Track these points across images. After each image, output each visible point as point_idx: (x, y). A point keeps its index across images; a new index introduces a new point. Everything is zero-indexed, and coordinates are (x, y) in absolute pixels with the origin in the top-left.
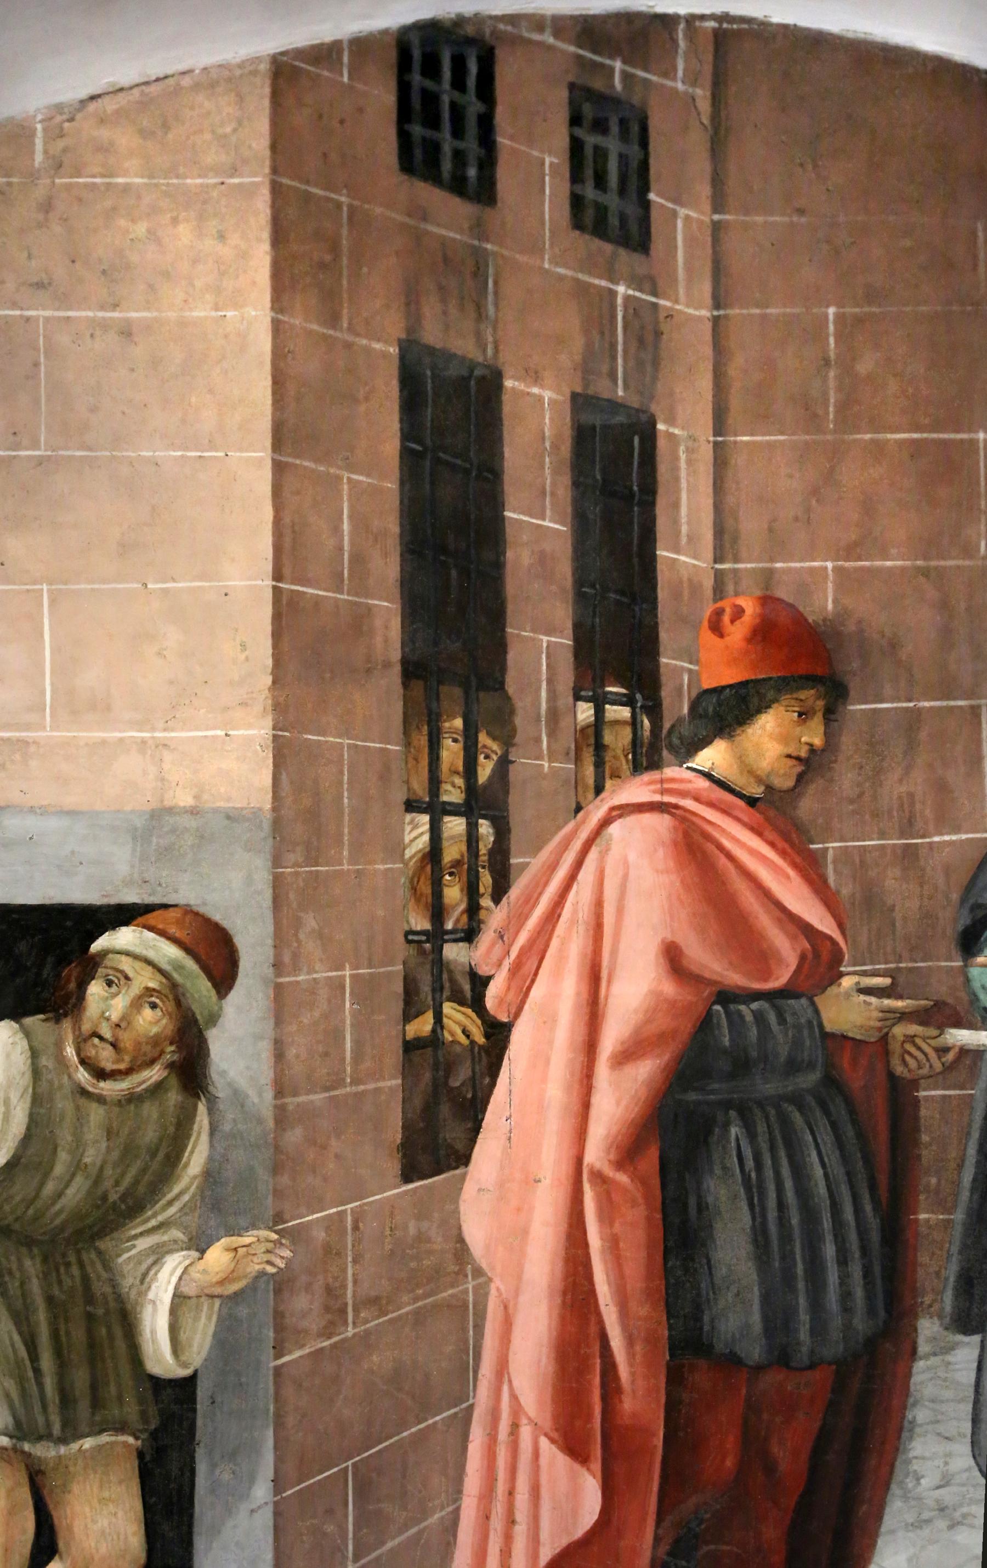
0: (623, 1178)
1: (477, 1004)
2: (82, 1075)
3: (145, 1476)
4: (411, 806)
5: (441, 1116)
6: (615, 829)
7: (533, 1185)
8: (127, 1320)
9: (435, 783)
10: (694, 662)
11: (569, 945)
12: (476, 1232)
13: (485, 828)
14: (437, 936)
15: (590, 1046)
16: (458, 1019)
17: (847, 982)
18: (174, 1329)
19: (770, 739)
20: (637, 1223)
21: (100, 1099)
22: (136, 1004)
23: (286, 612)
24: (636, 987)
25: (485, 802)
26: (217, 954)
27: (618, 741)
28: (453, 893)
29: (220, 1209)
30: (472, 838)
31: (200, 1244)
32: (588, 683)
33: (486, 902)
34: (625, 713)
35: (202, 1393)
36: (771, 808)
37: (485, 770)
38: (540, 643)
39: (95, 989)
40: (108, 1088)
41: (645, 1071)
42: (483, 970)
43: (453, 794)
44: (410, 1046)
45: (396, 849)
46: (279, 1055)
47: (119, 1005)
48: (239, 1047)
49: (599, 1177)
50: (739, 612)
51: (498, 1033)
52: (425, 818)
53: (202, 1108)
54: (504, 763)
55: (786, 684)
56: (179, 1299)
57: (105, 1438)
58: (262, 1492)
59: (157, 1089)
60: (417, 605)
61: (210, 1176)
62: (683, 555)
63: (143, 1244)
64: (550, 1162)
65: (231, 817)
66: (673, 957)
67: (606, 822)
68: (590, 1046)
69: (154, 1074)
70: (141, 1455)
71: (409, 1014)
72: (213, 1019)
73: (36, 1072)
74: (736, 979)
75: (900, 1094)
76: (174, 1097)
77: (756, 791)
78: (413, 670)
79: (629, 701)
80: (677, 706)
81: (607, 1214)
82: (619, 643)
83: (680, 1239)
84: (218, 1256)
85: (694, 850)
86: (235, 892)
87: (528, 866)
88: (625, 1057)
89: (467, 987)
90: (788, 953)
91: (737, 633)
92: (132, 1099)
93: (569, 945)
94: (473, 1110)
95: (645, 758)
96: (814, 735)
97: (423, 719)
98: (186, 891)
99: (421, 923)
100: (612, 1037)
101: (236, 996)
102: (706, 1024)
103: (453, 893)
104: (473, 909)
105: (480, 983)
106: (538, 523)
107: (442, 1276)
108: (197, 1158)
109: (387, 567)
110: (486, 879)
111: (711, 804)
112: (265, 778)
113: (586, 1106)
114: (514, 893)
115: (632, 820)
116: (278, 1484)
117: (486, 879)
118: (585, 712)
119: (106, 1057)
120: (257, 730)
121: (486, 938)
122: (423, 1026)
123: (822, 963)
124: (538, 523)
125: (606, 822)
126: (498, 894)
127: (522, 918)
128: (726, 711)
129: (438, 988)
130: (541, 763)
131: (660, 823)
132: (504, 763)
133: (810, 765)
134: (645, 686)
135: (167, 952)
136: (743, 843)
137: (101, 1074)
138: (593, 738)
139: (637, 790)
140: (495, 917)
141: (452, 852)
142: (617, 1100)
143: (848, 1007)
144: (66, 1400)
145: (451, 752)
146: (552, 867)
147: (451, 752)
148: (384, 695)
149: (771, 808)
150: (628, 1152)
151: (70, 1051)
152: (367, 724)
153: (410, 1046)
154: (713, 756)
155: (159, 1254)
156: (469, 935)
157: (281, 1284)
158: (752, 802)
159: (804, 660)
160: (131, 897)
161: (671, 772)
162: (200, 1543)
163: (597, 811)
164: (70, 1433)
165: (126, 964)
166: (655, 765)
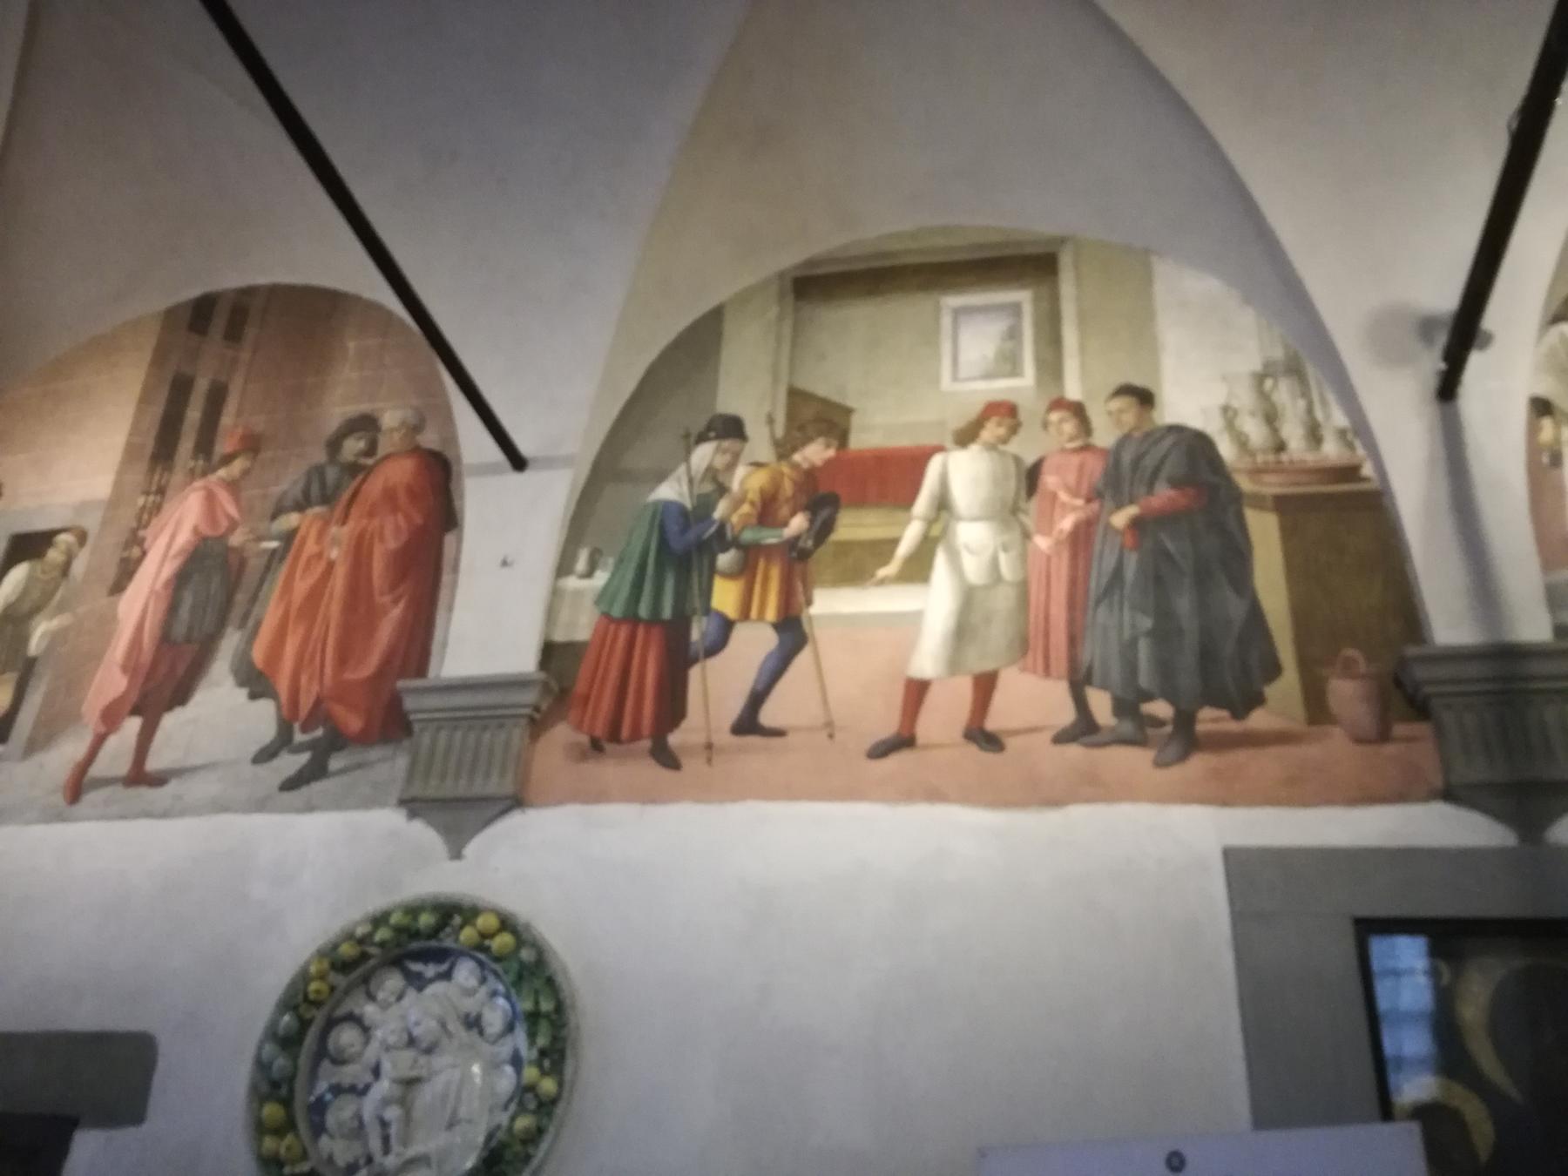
19: (238, 466)
20: (163, 606)
24: (184, 538)
25: (161, 491)
26: (82, 537)
27: (198, 471)
28: (146, 516)
32: (195, 457)
36: (233, 486)
38: (186, 445)
43: (154, 488)
48: (79, 567)
51: (144, 554)
64: (146, 590)
66: (196, 530)
82: (205, 446)
83: (173, 609)
85: (210, 498)
86: (91, 523)
90: (224, 524)
95: (204, 474)
97: (152, 470)
107: (108, 622)
123: (233, 526)
128: (227, 460)
136: (224, 497)
142: (168, 570)
143: (236, 540)
147: (156, 478)
148: (143, 466)
150: (167, 584)
152: (138, 475)
154: (222, 473)
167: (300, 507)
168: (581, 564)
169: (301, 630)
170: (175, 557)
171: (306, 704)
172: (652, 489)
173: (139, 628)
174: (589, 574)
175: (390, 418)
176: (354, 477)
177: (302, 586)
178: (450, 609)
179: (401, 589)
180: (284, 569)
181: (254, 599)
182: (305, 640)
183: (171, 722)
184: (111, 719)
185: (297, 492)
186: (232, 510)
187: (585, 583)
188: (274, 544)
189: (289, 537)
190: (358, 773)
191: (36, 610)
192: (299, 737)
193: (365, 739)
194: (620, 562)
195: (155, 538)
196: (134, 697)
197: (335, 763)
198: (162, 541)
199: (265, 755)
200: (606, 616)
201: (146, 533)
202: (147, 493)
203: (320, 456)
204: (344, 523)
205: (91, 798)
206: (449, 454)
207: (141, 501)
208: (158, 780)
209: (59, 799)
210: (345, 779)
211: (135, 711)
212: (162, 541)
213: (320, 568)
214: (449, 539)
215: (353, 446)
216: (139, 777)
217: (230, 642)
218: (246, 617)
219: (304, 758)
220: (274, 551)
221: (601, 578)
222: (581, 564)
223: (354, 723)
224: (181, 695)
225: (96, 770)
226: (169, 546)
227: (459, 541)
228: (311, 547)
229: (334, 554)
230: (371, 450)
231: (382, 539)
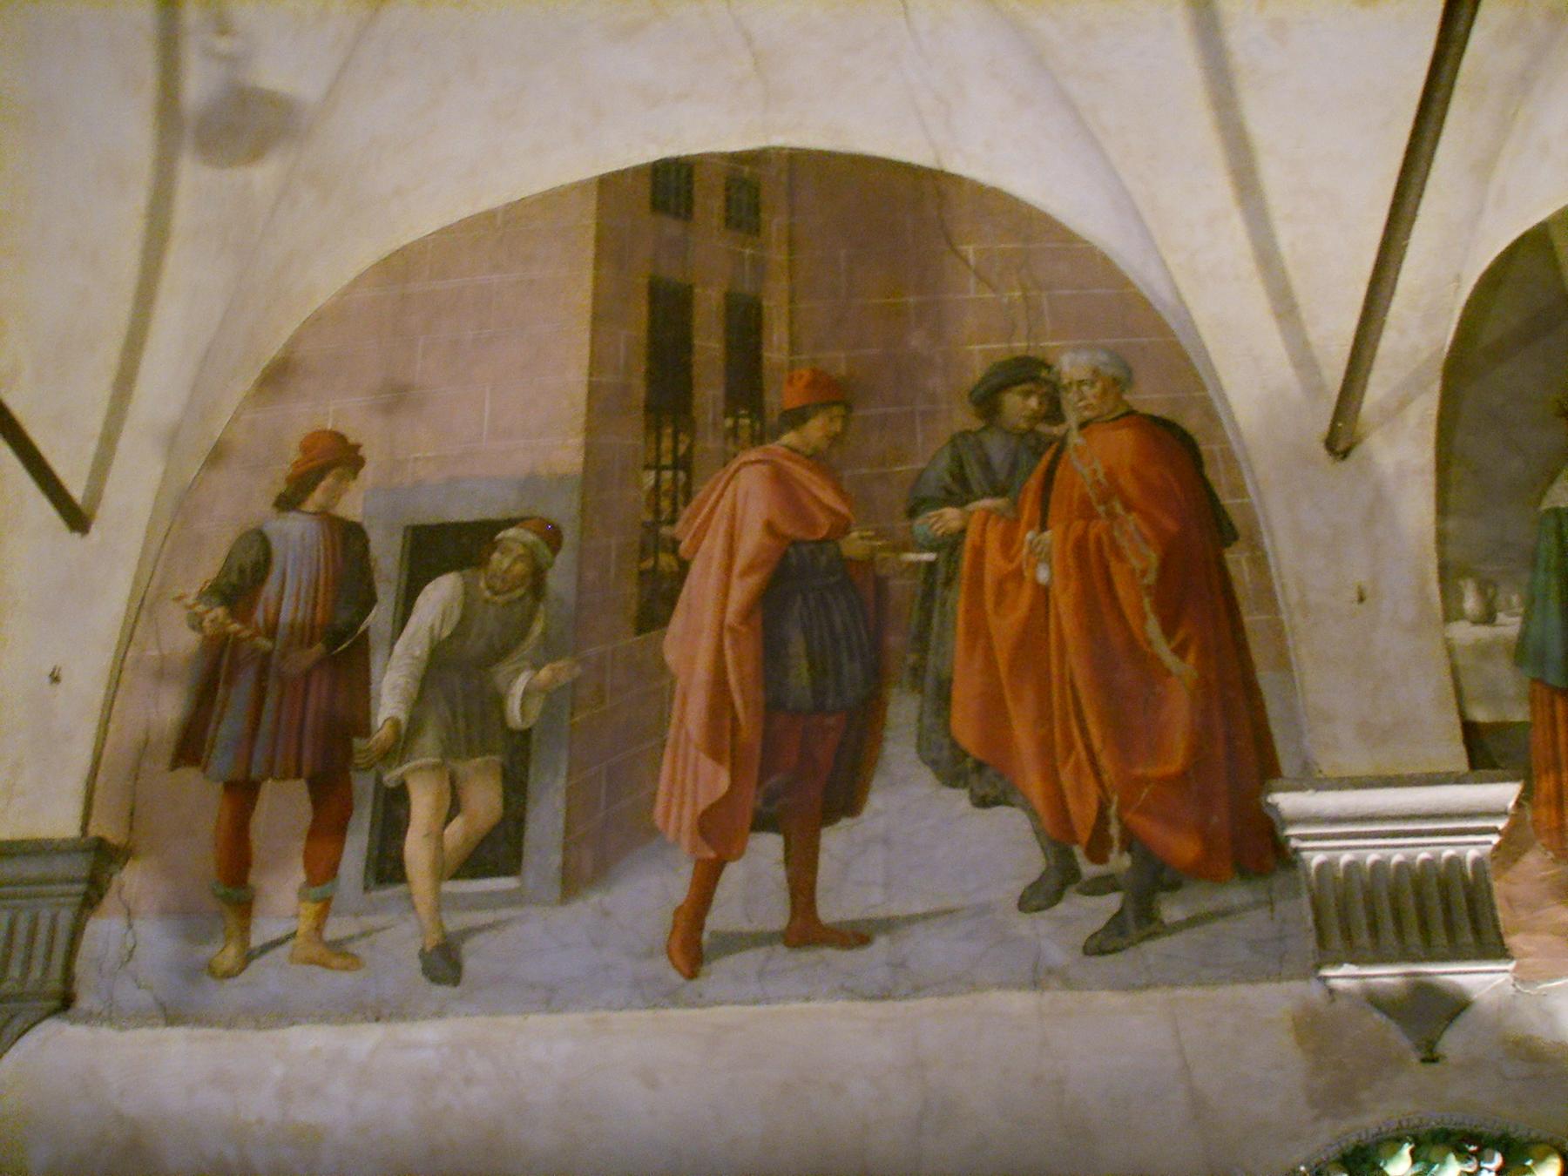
0: (744, 629)
1: (675, 551)
2: (487, 594)
3: (504, 776)
4: (647, 467)
5: (657, 601)
6: (743, 473)
7: (699, 638)
8: (499, 701)
9: (658, 457)
10: (781, 396)
11: (719, 526)
12: (671, 655)
13: (682, 475)
14: (657, 523)
15: (728, 569)
16: (666, 560)
17: (855, 534)
18: (523, 705)
19: (816, 430)
21: (495, 603)
22: (515, 561)
23: (593, 390)
24: (751, 540)
25: (683, 463)
26: (553, 537)
27: (744, 434)
28: (665, 504)
29: (550, 650)
30: (675, 480)
31: (537, 667)
32: (731, 411)
33: (680, 507)
34: (747, 421)
35: (534, 737)
36: (816, 460)
37: (682, 449)
38: (709, 392)
39: (496, 556)
40: (499, 599)
41: (754, 581)
42: (679, 537)
43: (667, 460)
44: (642, 573)
45: (639, 486)
46: (580, 579)
47: (506, 563)
48: (560, 579)
49: (732, 629)
50: (801, 376)
51: (684, 567)
52: (653, 474)
53: (542, 607)
54: (690, 448)
55: (826, 405)
56: (526, 693)
57: (487, 758)
58: (561, 782)
59: (521, 599)
60: (653, 380)
61: (544, 634)
62: (775, 351)
63: (511, 668)
65: (562, 478)
66: (770, 527)
67: (737, 471)
68: (728, 569)
69: (519, 592)
70: (503, 766)
71: (642, 560)
72: (551, 565)
73: (466, 593)
74: (800, 534)
75: (880, 584)
76: (529, 600)
77: (809, 452)
78: (651, 408)
79: (749, 416)
80: (773, 418)
81: (736, 643)
83: (772, 652)
84: (545, 673)
85: (780, 479)
87: (701, 490)
88: (745, 573)
89: (670, 545)
91: (800, 384)
92: (510, 603)
93: (719, 526)
94: (671, 601)
95: (758, 439)
96: (837, 426)
98: (540, 511)
99: (648, 517)
100: (740, 562)
101: (562, 555)
102: (785, 556)
103: (665, 504)
104: (675, 510)
105: (676, 543)
106: (709, 345)
108: (538, 628)
109: (641, 366)
110: (681, 498)
111: (789, 459)
112: (580, 459)
113: (726, 595)
114: (694, 504)
115: (752, 468)
116: (569, 775)
117: (681, 498)
118: (729, 422)
119: (498, 585)
120: (577, 441)
121: (680, 524)
122: (649, 563)
123: (842, 528)
124: (709, 345)
125: (737, 471)
126: (686, 503)
127: (696, 516)
128: (796, 418)
129: (656, 547)
130: (709, 443)
131: (764, 468)
132: (690, 448)
133: (835, 440)
134: (757, 410)
135: (530, 537)
137: (496, 593)
138: (734, 432)
139: (753, 455)
140: (685, 513)
141: (665, 486)
142: (740, 592)
143: (855, 544)
144: (469, 741)
145: (666, 444)
146: (713, 489)
147: (666, 444)
149: (816, 460)
150: (747, 615)
151: (482, 584)
152: (630, 436)
153: (642, 573)
154: (789, 438)
155: (518, 672)
156: (672, 521)
157: (575, 684)
158: (808, 457)
159: (832, 393)
160: (515, 514)
161: (769, 446)
162: (530, 805)
163: (734, 465)
164: (471, 754)
165: (511, 545)
166: (762, 443)
167: (958, 492)
168: (1471, 603)
169: (1029, 694)
170: (750, 569)
171: (1083, 814)
172: (1543, 493)
173: (719, 683)
174: (1488, 618)
175: (1071, 364)
176: (1039, 455)
177: (1005, 626)
178: (1283, 662)
179: (1181, 635)
180: (959, 600)
181: (921, 639)
182: (1044, 715)
183: (834, 841)
184: (719, 837)
185: (941, 471)
186: (828, 497)
187: (1484, 632)
188: (928, 557)
189: (951, 544)
190: (1220, 925)
191: (501, 652)
192: (1088, 869)
193: (1204, 872)
194: (1530, 603)
195: (698, 538)
196: (751, 800)
197: (1172, 910)
198: (714, 544)
199: (1038, 898)
200: (1538, 681)
201: (682, 531)
202: (659, 469)
203: (964, 418)
204: (1044, 527)
205: (720, 972)
206: (1191, 422)
207: (649, 479)
208: (855, 936)
209: (664, 969)
210: (1199, 934)
211: (762, 823)
212: (714, 544)
213: (1026, 597)
214: (1237, 560)
215: (1019, 405)
216: (806, 929)
217: (903, 711)
218: (917, 672)
219: (1111, 903)
220: (931, 566)
221: (1509, 626)
222: (1471, 603)
223: (1184, 848)
224: (844, 799)
225: (719, 919)
226: (730, 552)
227: (1259, 561)
228: (994, 563)
229: (1043, 575)
230: (1053, 411)
231: (1121, 557)
